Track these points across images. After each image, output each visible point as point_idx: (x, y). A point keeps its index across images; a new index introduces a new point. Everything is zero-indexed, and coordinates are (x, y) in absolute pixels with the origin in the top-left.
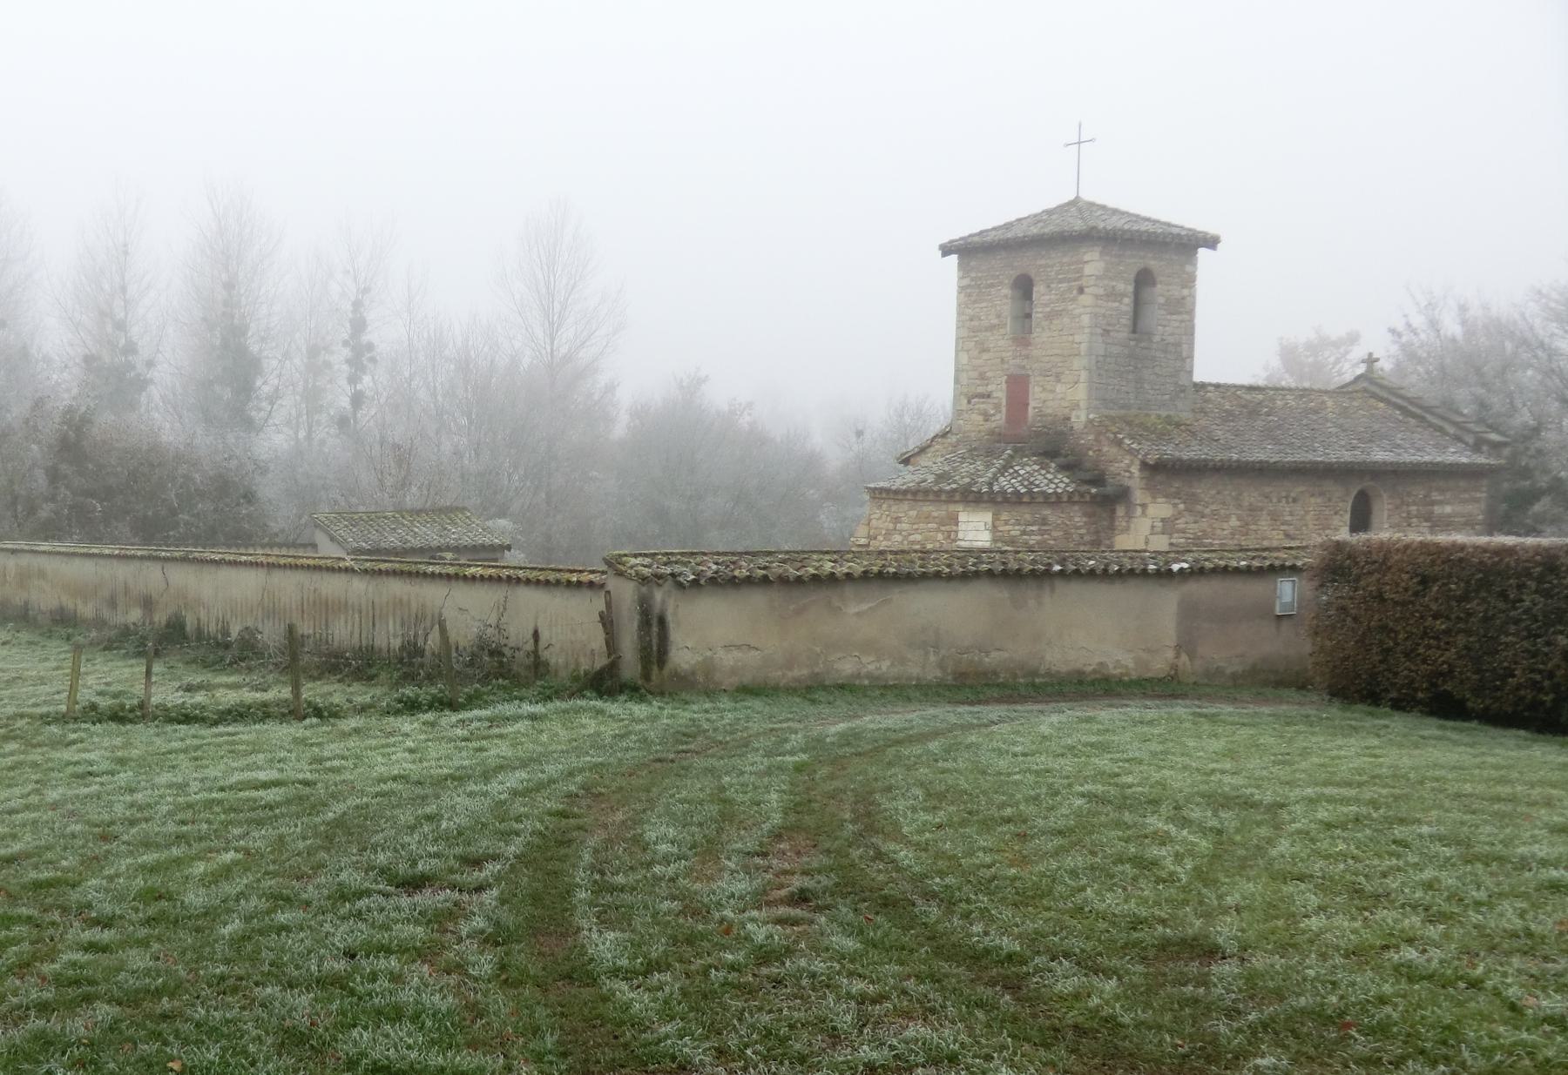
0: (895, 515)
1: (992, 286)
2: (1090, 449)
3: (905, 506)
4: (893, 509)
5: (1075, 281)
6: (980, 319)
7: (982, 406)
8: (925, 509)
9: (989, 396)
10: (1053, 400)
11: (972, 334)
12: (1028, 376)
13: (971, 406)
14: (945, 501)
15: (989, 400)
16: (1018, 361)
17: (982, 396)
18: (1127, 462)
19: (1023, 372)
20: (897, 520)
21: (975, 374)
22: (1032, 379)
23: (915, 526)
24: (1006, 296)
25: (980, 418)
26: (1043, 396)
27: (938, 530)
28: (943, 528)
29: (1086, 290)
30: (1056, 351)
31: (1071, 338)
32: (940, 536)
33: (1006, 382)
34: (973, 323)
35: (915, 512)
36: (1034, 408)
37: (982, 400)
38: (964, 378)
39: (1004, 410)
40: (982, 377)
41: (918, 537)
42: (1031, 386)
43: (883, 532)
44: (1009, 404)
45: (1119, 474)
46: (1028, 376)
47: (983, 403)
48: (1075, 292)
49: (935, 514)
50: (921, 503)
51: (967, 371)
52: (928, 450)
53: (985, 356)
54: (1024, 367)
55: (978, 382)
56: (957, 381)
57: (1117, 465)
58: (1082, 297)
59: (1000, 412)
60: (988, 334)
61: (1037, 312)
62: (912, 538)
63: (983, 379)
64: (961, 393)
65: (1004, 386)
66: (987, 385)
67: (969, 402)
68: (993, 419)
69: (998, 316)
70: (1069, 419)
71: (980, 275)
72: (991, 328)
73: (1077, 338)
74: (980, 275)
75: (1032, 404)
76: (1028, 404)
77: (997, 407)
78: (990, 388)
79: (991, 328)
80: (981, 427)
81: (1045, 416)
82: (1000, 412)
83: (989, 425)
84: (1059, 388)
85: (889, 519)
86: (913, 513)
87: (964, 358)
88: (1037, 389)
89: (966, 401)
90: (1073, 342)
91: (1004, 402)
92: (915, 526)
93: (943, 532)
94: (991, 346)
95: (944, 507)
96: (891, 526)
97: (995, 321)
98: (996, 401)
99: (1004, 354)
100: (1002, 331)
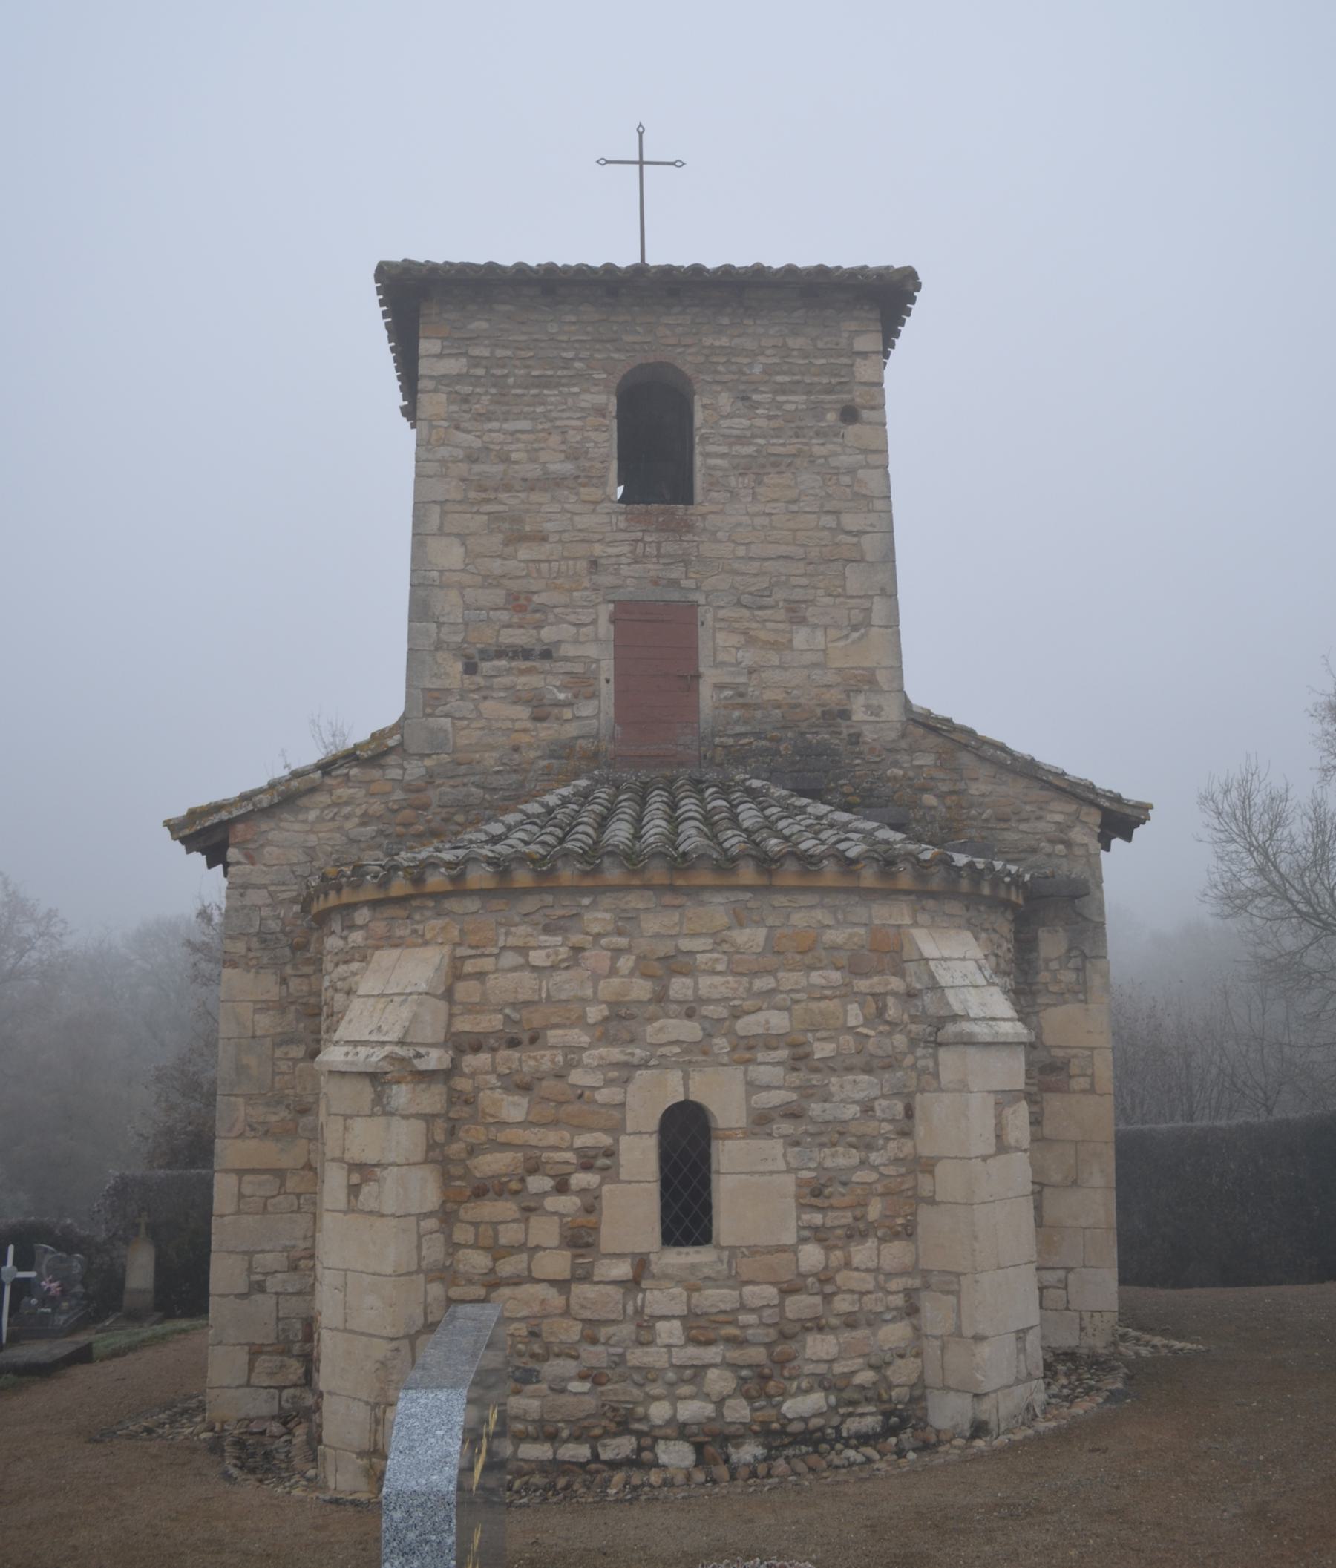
0: (665, 948)
1: (545, 383)
2: (924, 789)
3: (716, 910)
4: (652, 924)
5: (829, 392)
6: (505, 459)
7: (536, 681)
8: (799, 919)
9: (546, 654)
10: (781, 667)
11: (472, 495)
12: (694, 606)
13: (479, 680)
14: (907, 892)
15: (546, 665)
16: (652, 568)
17: (526, 654)
18: (1059, 818)
19: (675, 596)
20: (676, 964)
21: (497, 596)
22: (706, 615)
23: (762, 983)
24: (600, 411)
25: (523, 712)
26: (748, 657)
27: (846, 993)
28: (862, 985)
29: (866, 414)
30: (782, 550)
31: (828, 521)
32: (854, 1015)
33: (613, 620)
34: (477, 468)
35: (762, 933)
36: (720, 687)
37: (524, 665)
38: (449, 605)
39: (607, 691)
40: (518, 602)
41: (778, 1021)
42: (703, 634)
43: (595, 1013)
44: (622, 676)
45: (1034, 851)
46: (694, 606)
47: (522, 672)
48: (831, 417)
49: (835, 936)
50: (780, 900)
51: (462, 587)
52: (304, 801)
53: (525, 552)
54: (674, 583)
55: (505, 616)
56: (420, 610)
57: (1023, 827)
58: (851, 430)
59: (594, 695)
60: (535, 497)
61: (707, 455)
62: (747, 1025)
63: (520, 609)
64: (439, 645)
65: (605, 629)
66: (538, 627)
67: (470, 669)
68: (567, 714)
69: (574, 455)
70: (845, 714)
71: (500, 353)
72: (552, 483)
73: (850, 522)
74: (500, 353)
75: (710, 676)
76: (697, 676)
77: (582, 685)
78: (548, 634)
79: (552, 483)
80: (525, 739)
81: (758, 706)
82: (594, 695)
83: (547, 732)
84: (801, 637)
85: (626, 963)
86: (751, 938)
87: (450, 555)
88: (722, 638)
89: (459, 666)
90: (840, 529)
91: (607, 668)
92: (762, 983)
93: (860, 997)
94: (549, 526)
95: (860, 913)
96: (641, 989)
97: (568, 468)
98: (579, 668)
99: (598, 549)
100: (588, 493)
